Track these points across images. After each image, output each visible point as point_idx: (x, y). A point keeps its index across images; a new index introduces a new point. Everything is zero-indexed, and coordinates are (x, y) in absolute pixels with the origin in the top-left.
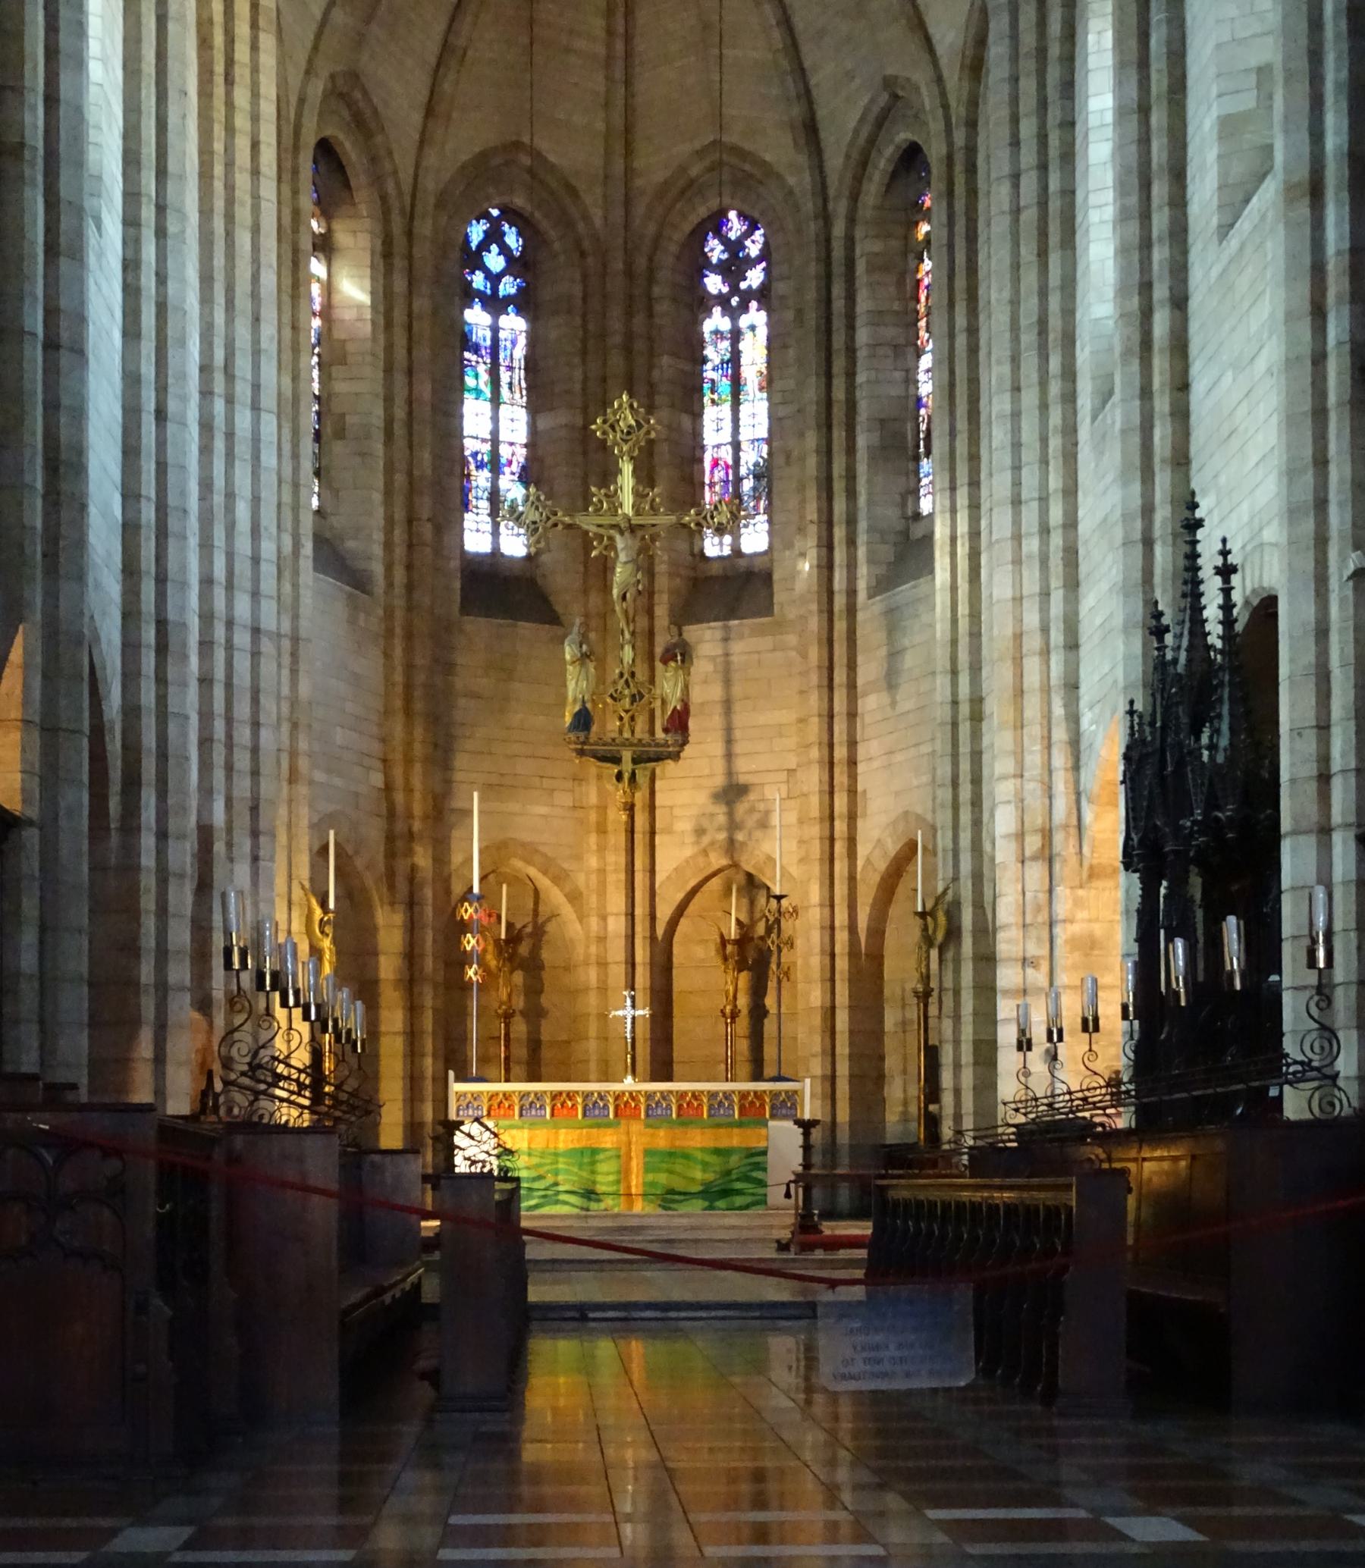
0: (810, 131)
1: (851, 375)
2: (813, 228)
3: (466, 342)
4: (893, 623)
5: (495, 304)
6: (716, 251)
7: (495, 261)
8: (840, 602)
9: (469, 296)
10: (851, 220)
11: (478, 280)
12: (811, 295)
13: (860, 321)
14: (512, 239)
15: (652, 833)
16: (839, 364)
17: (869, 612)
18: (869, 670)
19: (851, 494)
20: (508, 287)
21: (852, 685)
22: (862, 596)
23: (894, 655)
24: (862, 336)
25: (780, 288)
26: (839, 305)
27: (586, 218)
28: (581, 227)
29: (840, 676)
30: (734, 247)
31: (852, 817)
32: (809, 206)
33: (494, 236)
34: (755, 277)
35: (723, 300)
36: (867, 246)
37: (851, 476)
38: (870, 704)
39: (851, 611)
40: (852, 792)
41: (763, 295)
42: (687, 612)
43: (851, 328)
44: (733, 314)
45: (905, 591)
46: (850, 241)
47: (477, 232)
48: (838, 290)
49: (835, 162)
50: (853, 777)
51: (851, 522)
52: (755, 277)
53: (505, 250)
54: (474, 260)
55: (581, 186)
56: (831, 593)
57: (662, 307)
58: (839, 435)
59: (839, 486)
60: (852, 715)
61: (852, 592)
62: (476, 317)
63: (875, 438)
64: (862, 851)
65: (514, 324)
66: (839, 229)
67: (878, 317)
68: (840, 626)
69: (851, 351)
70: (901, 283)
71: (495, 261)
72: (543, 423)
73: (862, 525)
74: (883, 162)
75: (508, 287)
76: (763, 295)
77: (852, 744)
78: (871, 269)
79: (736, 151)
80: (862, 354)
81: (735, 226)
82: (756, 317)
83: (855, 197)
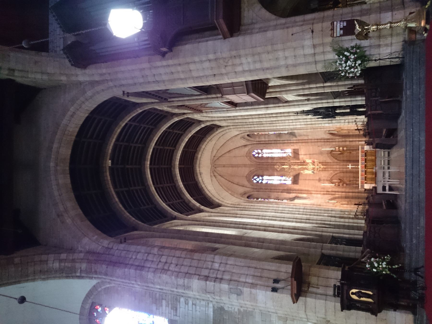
0: (245, 146)
1: (271, 141)
2: (255, 145)
3: (267, 183)
4: (300, 135)
5: (262, 180)
6: (257, 155)
7: (258, 180)
8: (297, 141)
9: (262, 183)
10: (254, 141)
11: (260, 181)
12: (262, 145)
13: (265, 140)
14: (256, 177)
15: (326, 162)
16: (270, 142)
17: (299, 138)
18: (306, 138)
19: (285, 140)
20: (261, 178)
21: (308, 140)
22: (297, 139)
23: (304, 135)
24: (267, 140)
25: (261, 149)
26: (264, 142)
27: (253, 170)
28: (254, 170)
29: (306, 141)
30: (256, 153)
31: (324, 139)
32: (253, 146)
33: (255, 179)
34: (260, 151)
35: (262, 154)
36: (257, 139)
37: (283, 141)
38: (310, 138)
39: (299, 140)
40: (321, 139)
41: (262, 150)
42: (298, 159)
43: (266, 141)
44: (264, 153)
45: (297, 135)
46: (256, 141)
47: (255, 181)
48: (262, 142)
49: (248, 143)
50: (319, 139)
51: (288, 140)
52: (260, 151)
53: (257, 178)
54: (258, 182)
55: (250, 170)
56: (296, 142)
57: (263, 161)
58: (278, 142)
59: (284, 142)
60: (311, 140)
61: (296, 140)
62: (264, 182)
63: (278, 138)
64: (328, 138)
65: (265, 177)
66: (255, 142)
67: (265, 138)
68: (300, 141)
69: (268, 141)
70: (261, 136)
71: (258, 180)
72: (276, 174)
73: (288, 139)
74: (248, 138)
75: (261, 178)
76: (262, 150)
77: (315, 139)
78: (259, 139)
79: (247, 154)
80: (269, 140)
81: (254, 153)
82: (264, 151)
83: (252, 141)
